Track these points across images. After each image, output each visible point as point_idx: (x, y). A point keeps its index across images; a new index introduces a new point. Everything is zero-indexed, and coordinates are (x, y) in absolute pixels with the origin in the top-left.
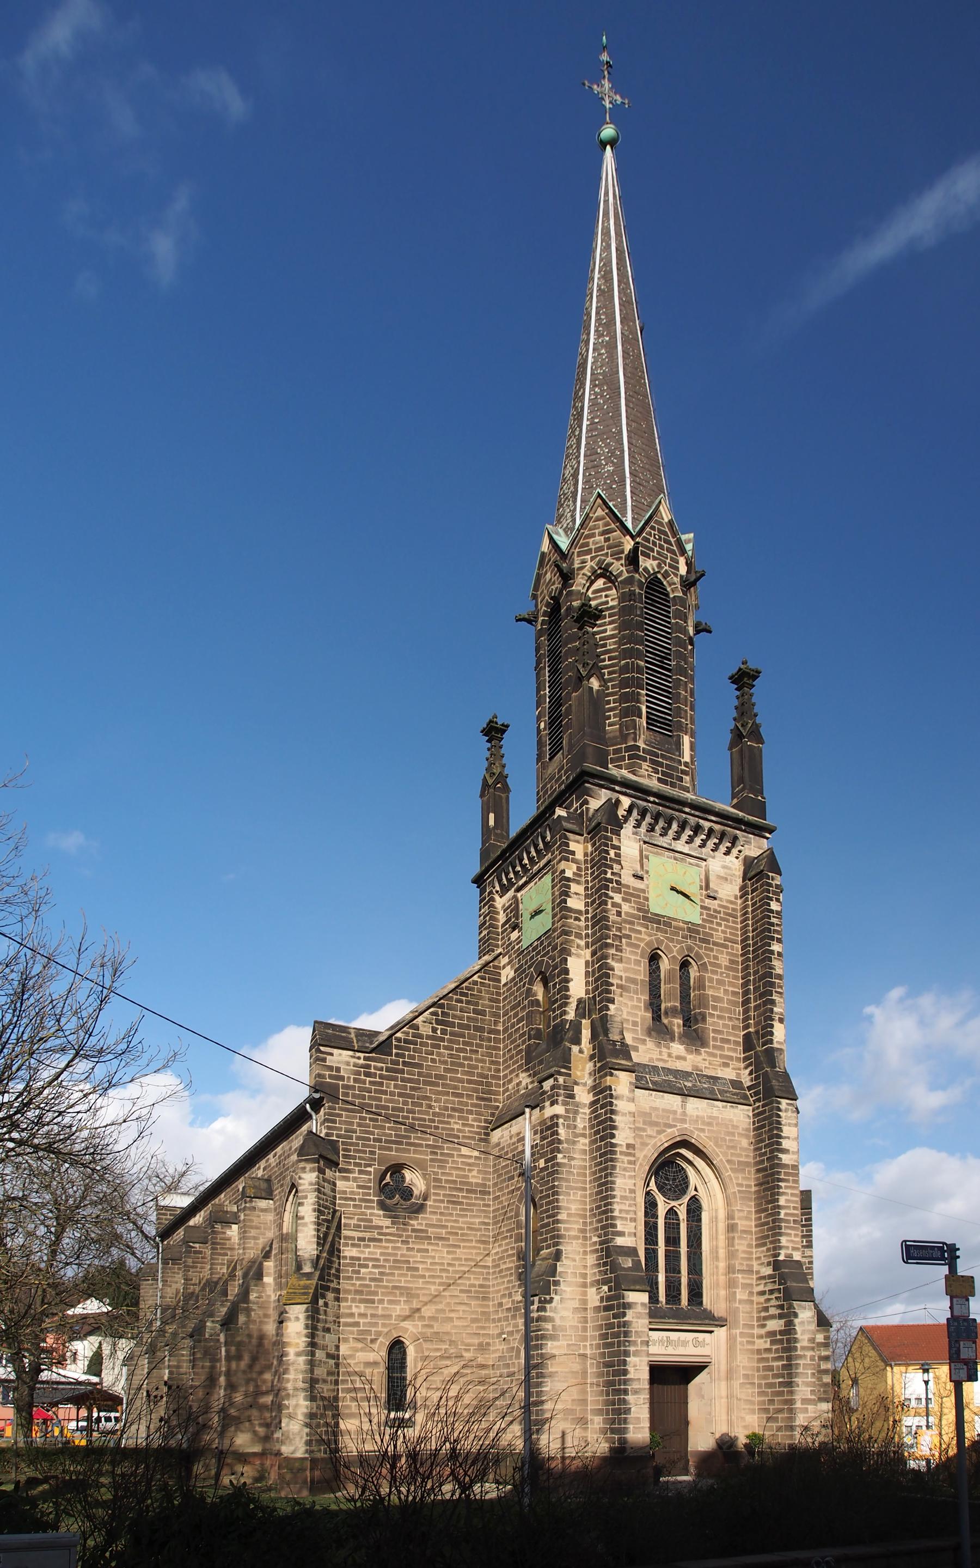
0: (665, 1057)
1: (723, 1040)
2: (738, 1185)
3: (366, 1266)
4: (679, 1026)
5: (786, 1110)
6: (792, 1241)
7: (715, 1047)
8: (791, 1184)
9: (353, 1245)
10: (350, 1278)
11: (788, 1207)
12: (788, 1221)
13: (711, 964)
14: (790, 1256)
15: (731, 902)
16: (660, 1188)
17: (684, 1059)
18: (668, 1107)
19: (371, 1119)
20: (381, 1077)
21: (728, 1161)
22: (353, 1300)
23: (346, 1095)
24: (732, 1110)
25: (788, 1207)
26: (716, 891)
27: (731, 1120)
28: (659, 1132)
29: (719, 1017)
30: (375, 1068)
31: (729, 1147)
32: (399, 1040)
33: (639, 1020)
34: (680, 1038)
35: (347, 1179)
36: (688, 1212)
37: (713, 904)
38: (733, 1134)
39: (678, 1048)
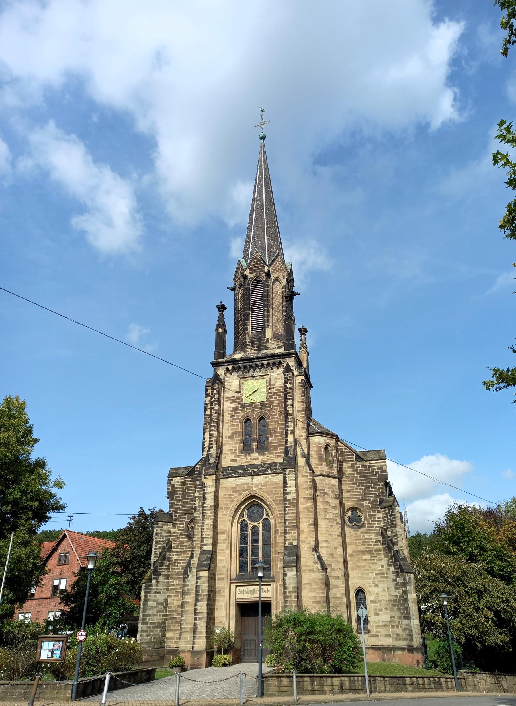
0: (249, 460)
1: (277, 446)
2: (279, 511)
3: (180, 563)
4: (255, 445)
5: (289, 474)
6: (292, 536)
7: (273, 450)
8: (291, 508)
9: (176, 555)
10: (174, 569)
11: (290, 520)
12: (290, 527)
15: (282, 387)
16: (249, 517)
17: (258, 459)
18: (245, 482)
19: (185, 502)
20: (190, 484)
21: (274, 501)
22: (175, 579)
23: (177, 494)
24: (276, 477)
25: (290, 520)
26: (275, 385)
27: (275, 482)
28: (240, 495)
29: (275, 436)
30: (188, 481)
31: (274, 494)
32: (197, 468)
33: (237, 448)
34: (256, 450)
35: (175, 528)
36: (263, 526)
37: (273, 390)
38: (277, 488)
39: (255, 455)
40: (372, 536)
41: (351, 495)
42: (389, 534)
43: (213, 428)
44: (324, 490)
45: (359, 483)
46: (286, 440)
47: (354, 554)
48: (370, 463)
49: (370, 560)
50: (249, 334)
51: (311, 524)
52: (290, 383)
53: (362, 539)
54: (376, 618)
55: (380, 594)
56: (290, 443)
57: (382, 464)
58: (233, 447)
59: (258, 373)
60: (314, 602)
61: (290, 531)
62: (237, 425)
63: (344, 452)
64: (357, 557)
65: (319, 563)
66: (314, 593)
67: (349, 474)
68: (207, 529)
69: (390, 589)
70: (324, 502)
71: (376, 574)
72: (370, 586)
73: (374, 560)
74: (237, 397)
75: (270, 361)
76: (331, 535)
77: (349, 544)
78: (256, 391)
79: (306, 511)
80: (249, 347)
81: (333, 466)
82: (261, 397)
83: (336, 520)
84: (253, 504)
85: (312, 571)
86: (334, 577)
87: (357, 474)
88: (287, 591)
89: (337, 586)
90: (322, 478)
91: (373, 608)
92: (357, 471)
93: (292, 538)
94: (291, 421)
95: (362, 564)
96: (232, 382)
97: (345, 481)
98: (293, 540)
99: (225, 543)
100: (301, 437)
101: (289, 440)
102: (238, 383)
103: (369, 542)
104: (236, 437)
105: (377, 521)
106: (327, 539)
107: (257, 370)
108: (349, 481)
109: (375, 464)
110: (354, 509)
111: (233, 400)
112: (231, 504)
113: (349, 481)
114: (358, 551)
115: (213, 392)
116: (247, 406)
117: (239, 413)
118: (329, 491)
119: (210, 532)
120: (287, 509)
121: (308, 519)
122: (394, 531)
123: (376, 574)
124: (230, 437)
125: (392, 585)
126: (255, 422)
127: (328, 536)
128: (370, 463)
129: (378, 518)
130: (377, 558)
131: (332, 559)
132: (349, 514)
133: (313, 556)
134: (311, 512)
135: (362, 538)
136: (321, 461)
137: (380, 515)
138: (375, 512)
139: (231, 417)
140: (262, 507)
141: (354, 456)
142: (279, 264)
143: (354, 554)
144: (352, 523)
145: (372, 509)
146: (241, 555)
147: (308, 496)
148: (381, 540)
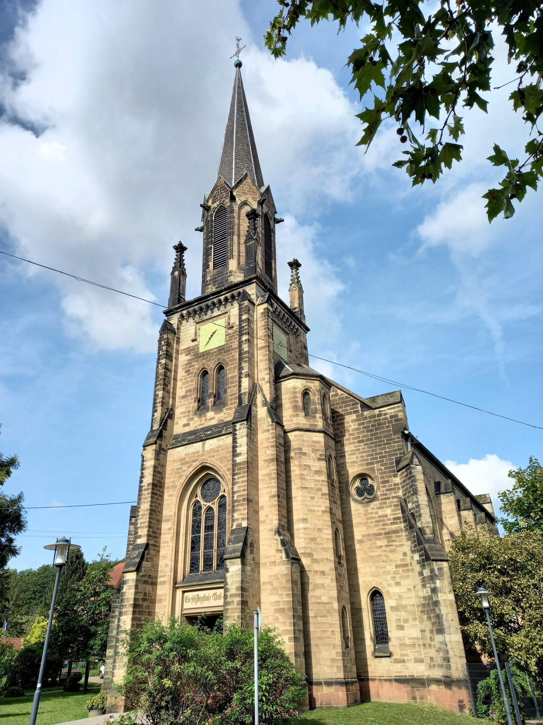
4: (211, 401)
6: (242, 514)
7: (231, 404)
8: (242, 475)
13: (231, 361)
14: (240, 525)
16: (204, 497)
17: (214, 418)
28: (189, 467)
33: (191, 409)
34: (212, 408)
36: (220, 506)
40: (388, 511)
41: (357, 458)
42: (410, 505)
43: (159, 387)
44: (301, 449)
45: (367, 440)
46: (240, 386)
47: (365, 539)
48: (380, 411)
49: (387, 546)
50: (210, 271)
51: (273, 496)
52: (245, 313)
53: (374, 518)
54: (400, 633)
55: (404, 596)
56: (245, 389)
57: (397, 409)
58: (186, 408)
59: (216, 312)
60: (276, 611)
61: (239, 508)
62: (192, 381)
63: (346, 402)
64: (368, 543)
65: (283, 551)
66: (276, 596)
67: (353, 430)
68: (143, 515)
69: (417, 588)
70: (300, 466)
71: (397, 566)
72: (389, 585)
73: (392, 545)
74: (193, 347)
75: (228, 295)
76: (312, 511)
77: (357, 526)
78: (214, 333)
79: (267, 478)
80: (210, 286)
81: (315, 417)
82: (219, 340)
83: (320, 490)
84: (205, 477)
85: (274, 563)
86: (316, 572)
87: (364, 428)
88: (228, 594)
89: (323, 586)
90: (297, 433)
91: (395, 618)
92: (363, 423)
93: (241, 517)
94: (246, 361)
95: (376, 554)
96: (188, 329)
97: (349, 439)
98: (243, 519)
99: (170, 533)
100: (263, 381)
101: (242, 384)
102: (194, 330)
103: (384, 520)
104: (190, 396)
105: (394, 489)
106: (305, 517)
107: (216, 309)
108: (354, 439)
109: (388, 411)
110: (363, 477)
111: (188, 351)
112: (179, 480)
113: (354, 439)
114: (369, 535)
115: (161, 344)
116: (204, 355)
117: (194, 365)
118: (308, 450)
119: (146, 519)
120: (236, 477)
121: (269, 490)
122: (415, 499)
123: (397, 566)
124: (184, 397)
125: (418, 580)
126: (212, 373)
127: (307, 512)
128: (380, 411)
129: (395, 485)
130: (397, 543)
131: (313, 546)
132: (357, 483)
133: (275, 542)
134: (274, 478)
135: (374, 515)
136: (296, 411)
137: (397, 480)
138: (390, 476)
139: (186, 372)
140: (218, 481)
141: (359, 405)
142: (248, 185)
143: (365, 539)
144: (362, 496)
145: (385, 473)
146: (193, 548)
147: (270, 457)
148: (400, 515)
